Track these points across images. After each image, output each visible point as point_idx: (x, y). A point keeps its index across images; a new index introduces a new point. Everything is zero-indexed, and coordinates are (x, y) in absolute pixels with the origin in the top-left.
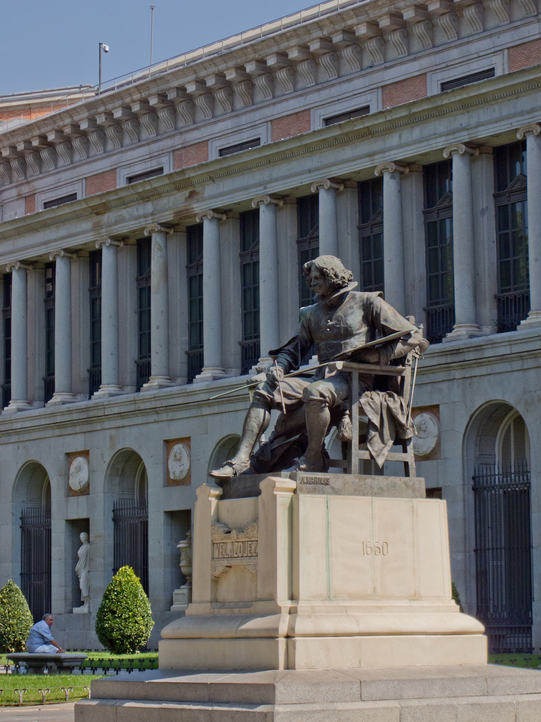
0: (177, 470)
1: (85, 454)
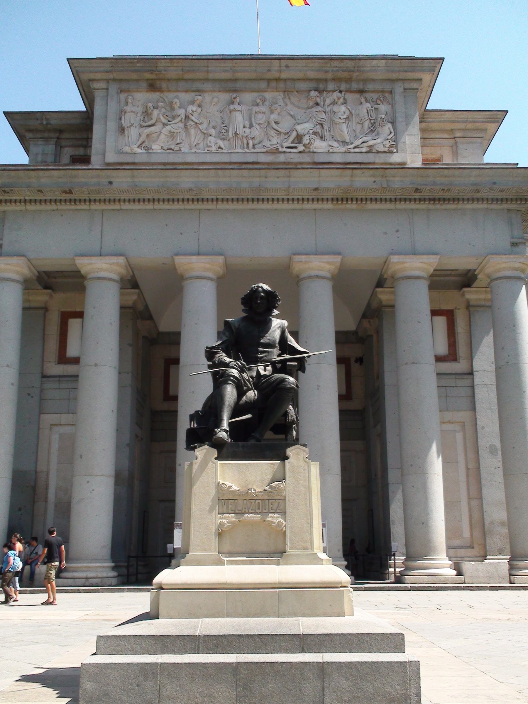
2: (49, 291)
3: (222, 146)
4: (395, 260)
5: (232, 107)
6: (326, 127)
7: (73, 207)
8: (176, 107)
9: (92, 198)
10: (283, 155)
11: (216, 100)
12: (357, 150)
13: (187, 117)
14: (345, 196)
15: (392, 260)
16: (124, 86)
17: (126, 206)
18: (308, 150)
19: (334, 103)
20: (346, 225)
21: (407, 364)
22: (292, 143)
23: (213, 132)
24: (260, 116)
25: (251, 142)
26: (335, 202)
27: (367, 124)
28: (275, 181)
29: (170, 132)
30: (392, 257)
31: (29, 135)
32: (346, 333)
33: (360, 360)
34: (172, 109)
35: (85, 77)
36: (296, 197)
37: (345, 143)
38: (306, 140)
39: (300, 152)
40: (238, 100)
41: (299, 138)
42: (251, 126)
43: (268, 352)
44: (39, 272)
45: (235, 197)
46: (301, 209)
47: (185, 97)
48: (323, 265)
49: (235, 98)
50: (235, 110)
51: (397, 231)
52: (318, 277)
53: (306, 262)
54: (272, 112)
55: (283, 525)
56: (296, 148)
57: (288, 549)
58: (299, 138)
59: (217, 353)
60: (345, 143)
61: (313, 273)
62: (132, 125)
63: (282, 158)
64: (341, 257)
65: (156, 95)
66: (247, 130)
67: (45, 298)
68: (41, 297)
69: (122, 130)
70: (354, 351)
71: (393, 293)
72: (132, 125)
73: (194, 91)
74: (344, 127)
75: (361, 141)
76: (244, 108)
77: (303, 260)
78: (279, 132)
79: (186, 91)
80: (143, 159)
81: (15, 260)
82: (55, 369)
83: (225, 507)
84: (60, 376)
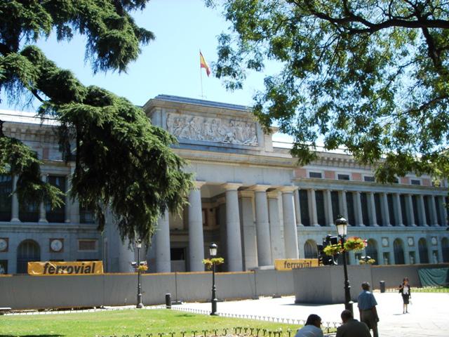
18: (231, 143)
19: (238, 125)
32: (207, 199)
38: (231, 139)
41: (228, 138)
58: (228, 138)
63: (222, 145)
65: (178, 115)
70: (209, 206)
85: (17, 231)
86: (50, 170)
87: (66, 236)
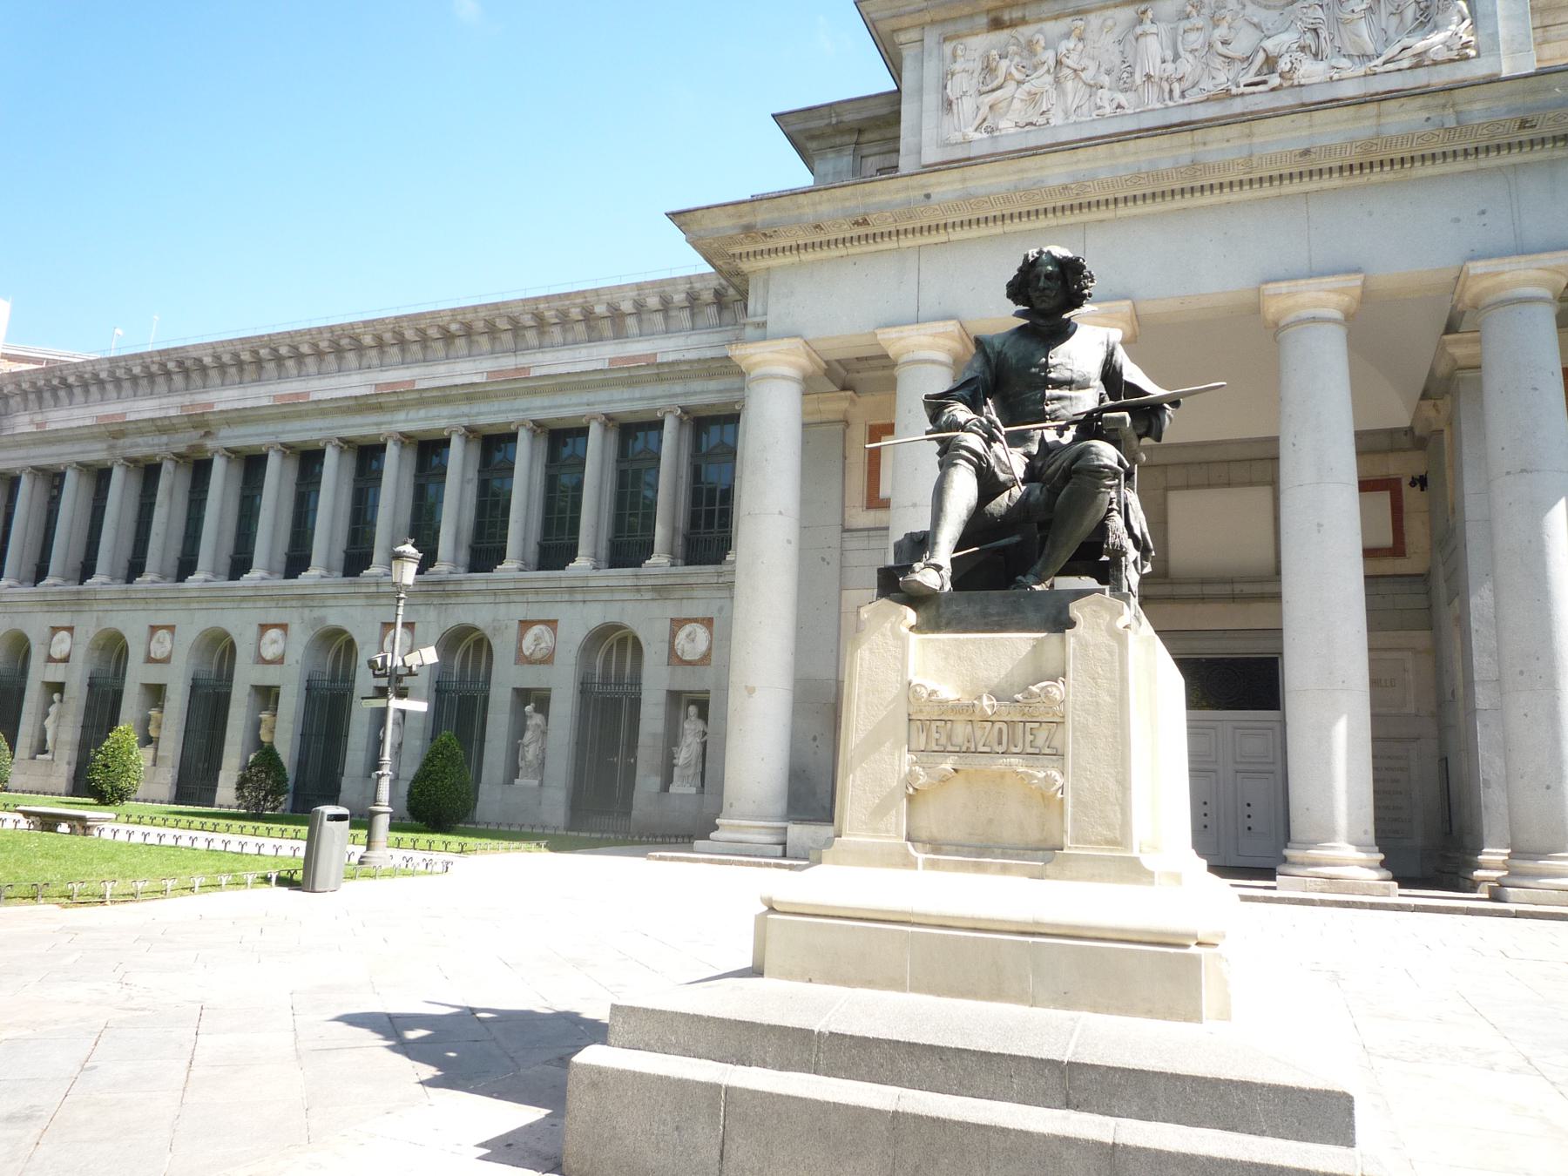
0: (158, 651)
1: (70, 629)
2: (849, 393)
3: (1124, 102)
4: (1479, 271)
5: (1139, 30)
6: (1324, 33)
7: (873, 248)
8: (1039, 49)
9: (902, 228)
10: (1238, 100)
11: (1110, 23)
12: (1390, 66)
13: (1059, 63)
14: (1366, 160)
15: (1472, 272)
16: (950, 29)
17: (958, 234)
20: (1370, 214)
21: (1508, 473)
22: (1257, 75)
23: (1106, 80)
24: (1192, 36)
25: (1177, 88)
26: (1346, 174)
27: (1410, 13)
28: (1221, 148)
29: (1029, 93)
30: (1470, 265)
31: (812, 145)
33: (1421, 482)
34: (1033, 53)
35: (885, 27)
36: (1266, 174)
37: (1366, 57)
38: (1284, 65)
39: (1273, 90)
40: (1150, 14)
41: (1271, 63)
42: (1176, 57)
43: (1071, 398)
44: (827, 362)
45: (1148, 191)
46: (1280, 196)
47: (1053, 28)
48: (1323, 295)
49: (1144, 12)
50: (1144, 34)
51: (1483, 212)
52: (1314, 320)
53: (1290, 294)
54: (1216, 26)
55: (1058, 784)
56: (1264, 82)
57: (1067, 841)
58: (1271, 63)
59: (946, 406)
60: (1366, 57)
61: (1305, 313)
62: (965, 93)
63: (1237, 106)
64: (1361, 276)
65: (1003, 36)
66: (1170, 67)
67: (845, 405)
68: (837, 404)
69: (948, 105)
71: (1478, 341)
72: (965, 93)
73: (1070, 15)
74: (1363, 28)
75: (1398, 48)
76: (1162, 27)
77: (1284, 291)
78: (1230, 60)
79: (1056, 18)
80: (986, 149)
81: (785, 344)
82: (863, 518)
83: (923, 737)
84: (869, 530)
85: (579, 597)
86: (686, 394)
87: (721, 609)
